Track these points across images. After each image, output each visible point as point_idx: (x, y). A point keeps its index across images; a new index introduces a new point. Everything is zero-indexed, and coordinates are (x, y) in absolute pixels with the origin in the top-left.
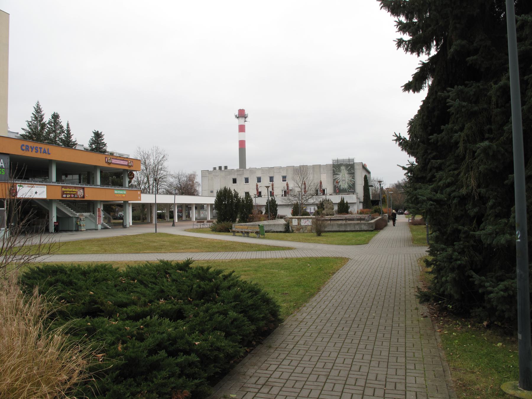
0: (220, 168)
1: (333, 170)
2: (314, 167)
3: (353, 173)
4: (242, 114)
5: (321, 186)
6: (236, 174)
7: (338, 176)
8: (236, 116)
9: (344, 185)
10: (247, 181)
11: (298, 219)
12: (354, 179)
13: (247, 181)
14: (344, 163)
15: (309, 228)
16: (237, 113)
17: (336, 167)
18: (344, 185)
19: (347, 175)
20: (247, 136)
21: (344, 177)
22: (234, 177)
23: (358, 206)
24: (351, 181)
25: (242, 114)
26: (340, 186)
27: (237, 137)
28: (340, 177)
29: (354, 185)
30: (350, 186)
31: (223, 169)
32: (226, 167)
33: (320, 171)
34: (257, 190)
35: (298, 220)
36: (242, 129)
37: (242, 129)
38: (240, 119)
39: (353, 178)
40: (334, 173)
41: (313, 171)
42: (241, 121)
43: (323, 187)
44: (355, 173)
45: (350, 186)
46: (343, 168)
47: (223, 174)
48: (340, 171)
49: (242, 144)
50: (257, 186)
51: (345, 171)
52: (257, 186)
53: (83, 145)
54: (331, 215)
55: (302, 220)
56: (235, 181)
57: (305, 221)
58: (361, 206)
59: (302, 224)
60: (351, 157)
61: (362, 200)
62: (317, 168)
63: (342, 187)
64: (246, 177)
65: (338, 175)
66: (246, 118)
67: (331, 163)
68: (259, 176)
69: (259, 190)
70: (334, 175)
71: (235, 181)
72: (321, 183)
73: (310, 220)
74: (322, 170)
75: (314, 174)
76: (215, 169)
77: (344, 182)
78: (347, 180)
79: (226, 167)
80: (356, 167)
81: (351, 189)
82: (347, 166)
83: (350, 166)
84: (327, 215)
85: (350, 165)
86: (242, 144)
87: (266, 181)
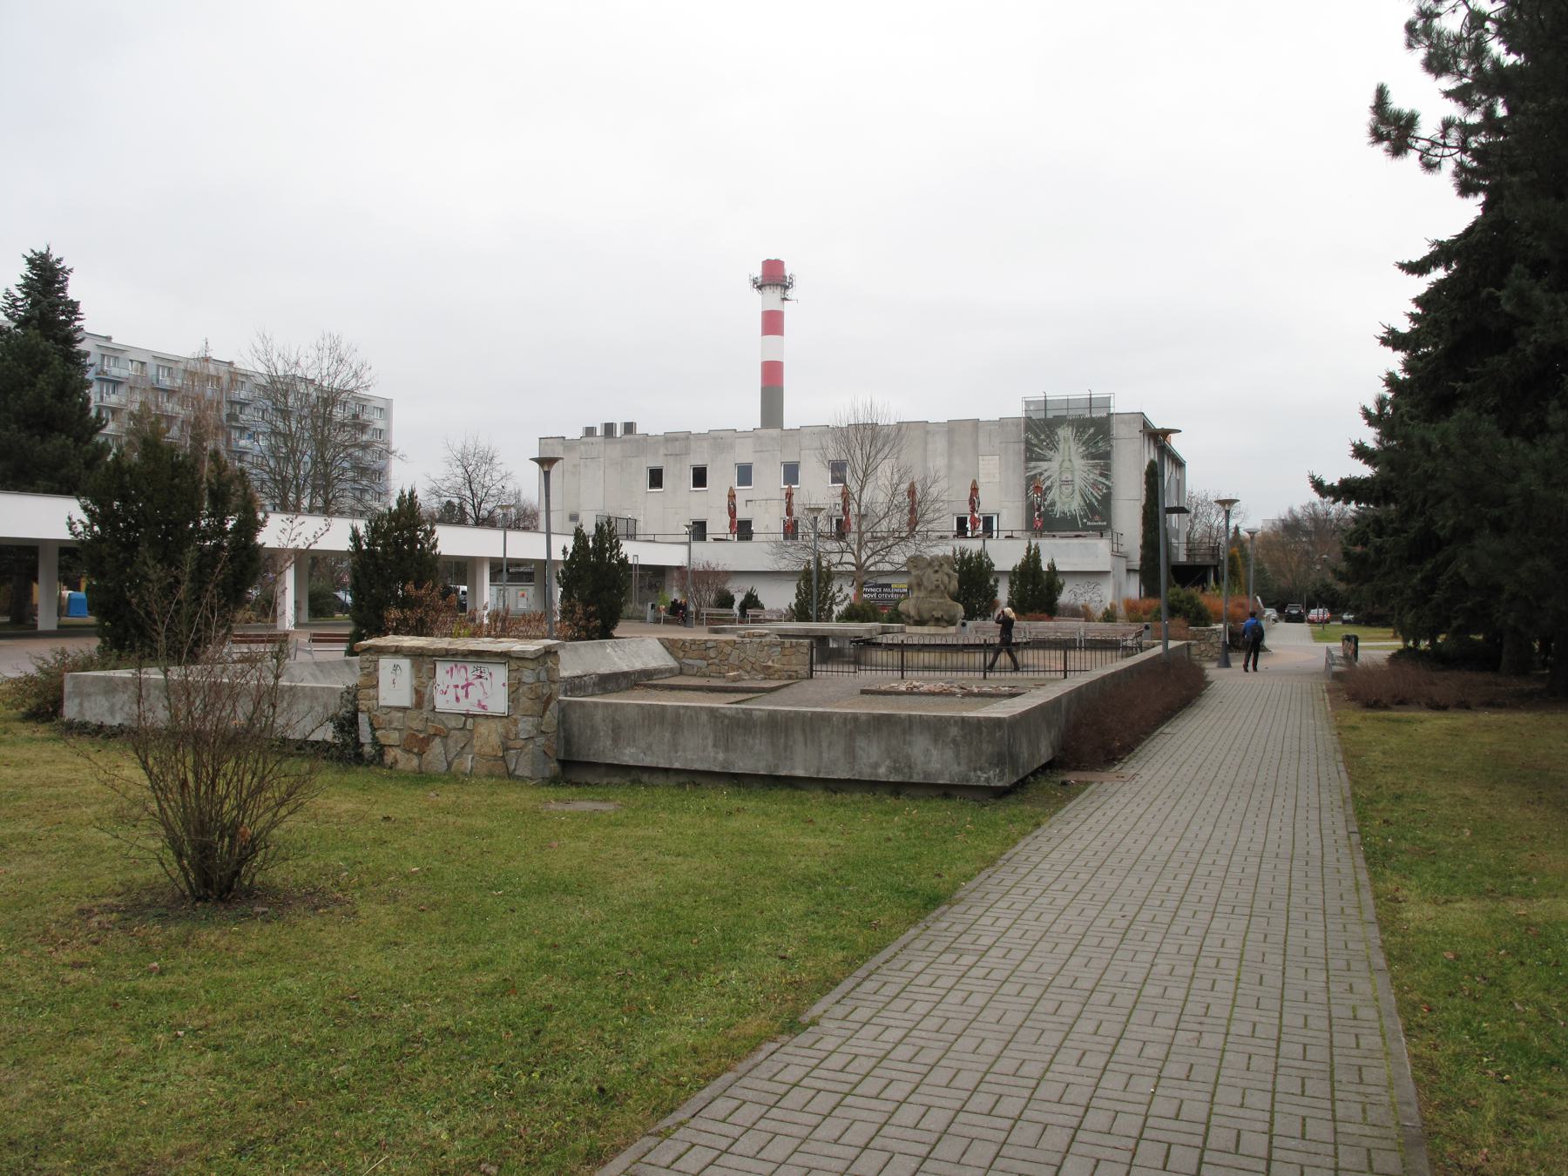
0: (609, 428)
1: (1027, 442)
2: (952, 428)
3: (1106, 456)
4: (773, 277)
5: (973, 502)
6: (662, 451)
7: (1044, 465)
9: (1068, 502)
10: (700, 477)
11: (416, 655)
12: (1107, 477)
13: (700, 477)
14: (1073, 414)
15: (489, 737)
16: (758, 272)
17: (1040, 430)
18: (1068, 502)
19: (1079, 464)
20: (790, 348)
21: (1068, 470)
22: (655, 464)
23: (1118, 588)
24: (1095, 485)
25: (773, 277)
26: (1053, 504)
27: (755, 349)
28: (1052, 468)
29: (1107, 500)
30: (1090, 506)
31: (619, 432)
32: (629, 428)
33: (976, 445)
34: (732, 513)
35: (417, 668)
36: (772, 323)
37: (772, 323)
38: (768, 291)
39: (1106, 472)
40: (1032, 454)
41: (951, 443)
42: (772, 299)
43: (986, 507)
44: (1114, 456)
45: (1090, 506)
46: (1064, 433)
47: (614, 451)
48: (1053, 446)
49: (772, 374)
50: (732, 496)
51: (1073, 447)
52: (732, 496)
54: (938, 621)
55: (442, 669)
56: (656, 478)
57: (460, 677)
58: (1133, 588)
59: (443, 703)
60: (1098, 392)
61: (1136, 562)
62: (965, 433)
63: (1058, 508)
64: (699, 463)
65: (1044, 459)
66: (786, 288)
67: (1018, 411)
68: (745, 460)
69: (741, 514)
70: (1028, 460)
71: (656, 478)
72: (975, 490)
73: (499, 675)
74: (982, 440)
75: (950, 457)
76: (590, 431)
77: (1067, 490)
78: (1079, 483)
79: (629, 428)
80: (1118, 430)
81: (1096, 517)
82: (1081, 425)
83: (1094, 429)
84: (921, 622)
85: (1093, 422)
86: (772, 374)
87: (769, 481)
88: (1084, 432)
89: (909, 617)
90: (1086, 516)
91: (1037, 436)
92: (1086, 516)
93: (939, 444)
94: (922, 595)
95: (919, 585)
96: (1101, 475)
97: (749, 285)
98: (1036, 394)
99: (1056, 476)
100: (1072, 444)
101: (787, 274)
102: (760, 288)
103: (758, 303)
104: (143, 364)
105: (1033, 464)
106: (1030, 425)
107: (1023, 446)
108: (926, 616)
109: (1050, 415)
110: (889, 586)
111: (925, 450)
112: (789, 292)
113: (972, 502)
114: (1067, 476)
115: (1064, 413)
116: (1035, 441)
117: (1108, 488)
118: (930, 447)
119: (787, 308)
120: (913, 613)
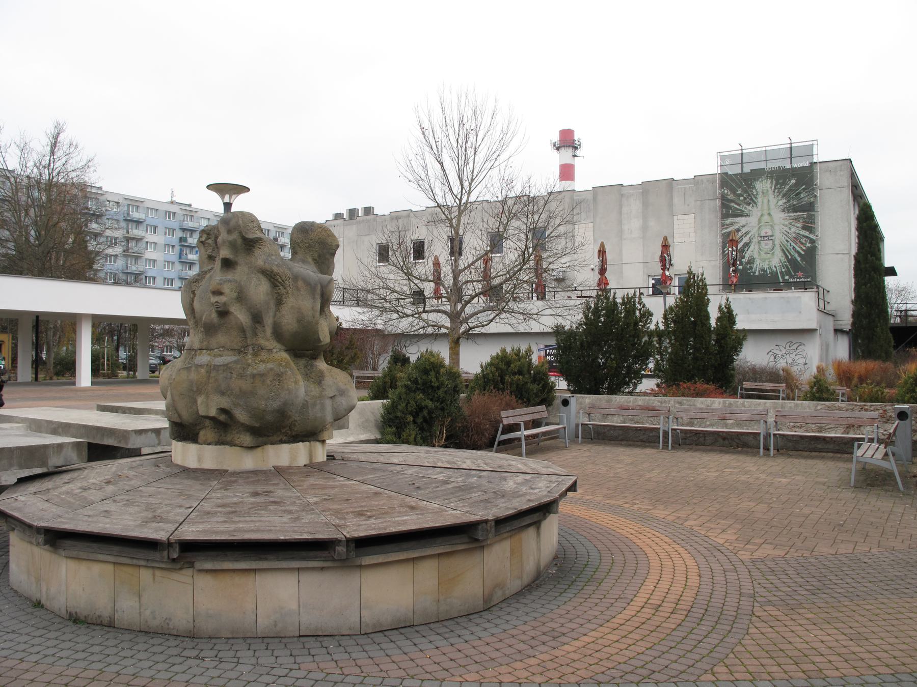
0: (352, 213)
1: (723, 198)
2: (647, 188)
3: (810, 208)
7: (741, 221)
8: (554, 145)
9: (767, 258)
12: (810, 230)
14: (771, 165)
16: (556, 138)
17: (735, 188)
18: (767, 258)
19: (779, 217)
21: (768, 227)
23: (825, 348)
24: (797, 239)
26: (751, 261)
28: (749, 224)
29: (811, 255)
30: (792, 261)
32: (368, 211)
33: (671, 205)
38: (563, 150)
39: (809, 225)
40: (728, 210)
41: (645, 205)
44: (818, 206)
45: (792, 261)
46: (763, 186)
53: (190, 205)
58: (841, 350)
60: (800, 138)
61: (846, 321)
62: (658, 194)
63: (758, 266)
66: (576, 148)
67: (712, 167)
70: (724, 216)
72: (666, 246)
75: (645, 218)
76: (338, 216)
77: (766, 246)
78: (779, 237)
80: (822, 179)
81: (801, 271)
82: (780, 176)
83: (797, 181)
85: (793, 172)
88: (784, 183)
90: (788, 273)
91: (734, 191)
92: (788, 273)
93: (634, 206)
96: (804, 228)
97: (551, 147)
98: (731, 147)
99: (754, 231)
100: (771, 197)
101: (576, 138)
102: (558, 149)
103: (556, 160)
104: (118, 203)
105: (729, 221)
106: (726, 180)
107: (718, 203)
109: (747, 169)
111: (620, 213)
112: (578, 152)
113: (663, 260)
114: (766, 231)
115: (761, 166)
116: (731, 197)
117: (812, 241)
118: (625, 210)
119: (577, 162)
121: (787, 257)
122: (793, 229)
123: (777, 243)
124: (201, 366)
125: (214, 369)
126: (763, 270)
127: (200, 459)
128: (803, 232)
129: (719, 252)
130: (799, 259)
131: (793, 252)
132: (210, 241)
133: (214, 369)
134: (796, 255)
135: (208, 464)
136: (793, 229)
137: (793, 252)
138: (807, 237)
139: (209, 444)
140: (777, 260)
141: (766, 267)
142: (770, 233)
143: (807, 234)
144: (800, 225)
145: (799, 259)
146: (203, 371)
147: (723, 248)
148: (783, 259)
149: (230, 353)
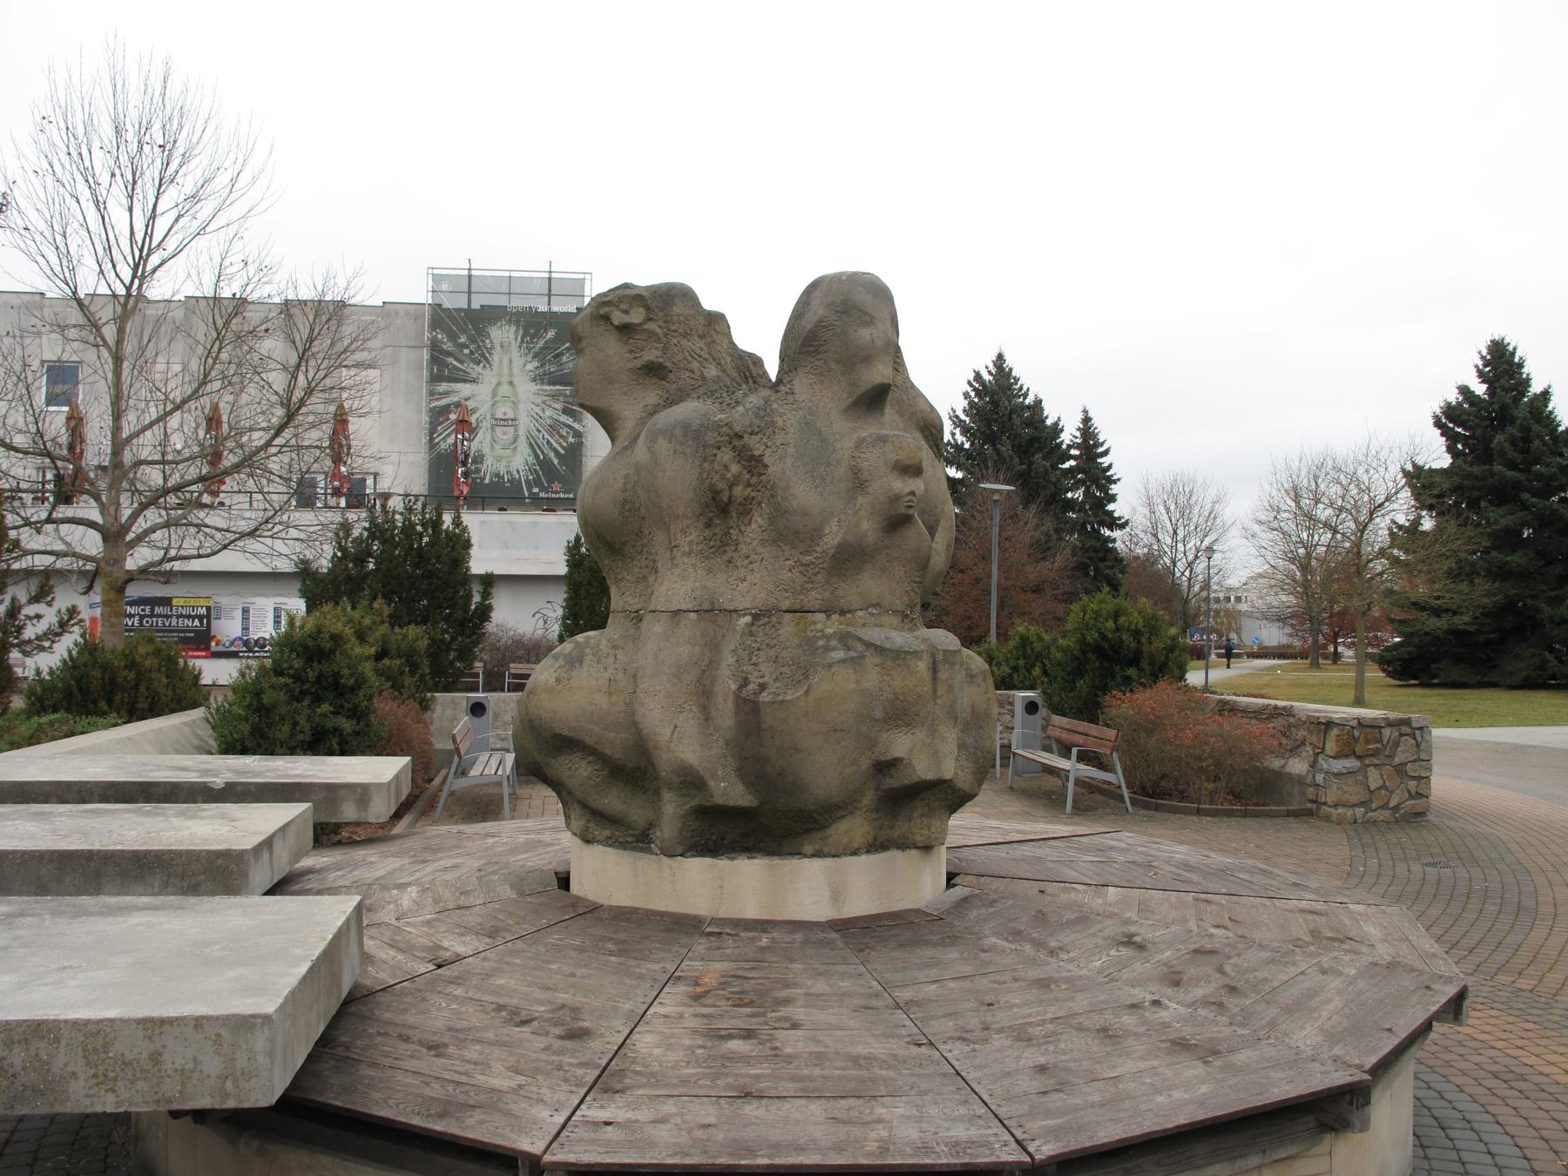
1: (435, 347)
7: (464, 389)
14: (518, 303)
19: (527, 390)
24: (554, 428)
26: (479, 459)
28: (478, 394)
30: (545, 464)
40: (441, 369)
45: (545, 464)
46: (502, 335)
48: (482, 357)
51: (518, 361)
65: (465, 379)
67: (419, 293)
70: (435, 379)
78: (525, 424)
88: (536, 336)
89: (634, 769)
90: (538, 482)
91: (453, 337)
92: (538, 482)
94: (750, 584)
95: (720, 510)
96: (566, 411)
98: (454, 262)
99: (484, 409)
100: (515, 354)
105: (443, 387)
106: (440, 317)
107: (426, 354)
108: (825, 769)
109: (476, 305)
110: (167, 602)
114: (504, 410)
115: (501, 301)
116: (448, 346)
117: (578, 434)
120: (684, 741)
121: (537, 456)
122: (548, 413)
123: (522, 431)
124: (916, 654)
125: (946, 660)
126: (497, 475)
127: (837, 896)
128: (564, 419)
129: (425, 440)
130: (556, 462)
131: (546, 449)
132: (651, 326)
133: (946, 660)
134: (552, 455)
135: (860, 905)
136: (548, 413)
137: (546, 449)
138: (569, 426)
139: (855, 853)
140: (522, 461)
141: (503, 470)
142: (511, 415)
143: (569, 421)
144: (559, 406)
145: (556, 462)
146: (922, 666)
147: (432, 431)
148: (531, 459)
149: (895, 620)
